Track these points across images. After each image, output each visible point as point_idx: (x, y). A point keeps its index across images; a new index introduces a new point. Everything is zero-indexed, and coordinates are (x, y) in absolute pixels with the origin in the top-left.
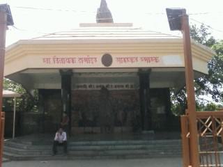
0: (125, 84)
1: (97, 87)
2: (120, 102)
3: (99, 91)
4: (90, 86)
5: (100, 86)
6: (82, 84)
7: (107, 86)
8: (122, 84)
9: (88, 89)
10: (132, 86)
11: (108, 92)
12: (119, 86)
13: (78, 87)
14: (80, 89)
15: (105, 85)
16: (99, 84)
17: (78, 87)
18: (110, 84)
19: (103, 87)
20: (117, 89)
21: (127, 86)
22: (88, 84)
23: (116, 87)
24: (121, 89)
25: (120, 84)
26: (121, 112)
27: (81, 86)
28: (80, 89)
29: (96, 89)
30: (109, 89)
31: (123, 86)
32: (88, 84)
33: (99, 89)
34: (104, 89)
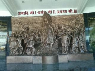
0: (68, 9)
1: (39, 13)
2: (63, 28)
3: (42, 17)
4: (31, 13)
5: (42, 12)
6: (24, 11)
7: (49, 12)
8: (65, 9)
9: (30, 15)
10: (75, 11)
13: (20, 13)
15: (47, 10)
16: (41, 10)
17: (20, 13)
18: (52, 10)
19: (46, 12)
20: (60, 14)
21: (70, 11)
22: (29, 11)
23: (59, 12)
24: (64, 14)
25: (62, 9)
26: (65, 39)
27: (22, 13)
28: (21, 15)
29: (38, 15)
30: (52, 15)
31: (66, 11)
32: (29, 11)
33: (42, 15)
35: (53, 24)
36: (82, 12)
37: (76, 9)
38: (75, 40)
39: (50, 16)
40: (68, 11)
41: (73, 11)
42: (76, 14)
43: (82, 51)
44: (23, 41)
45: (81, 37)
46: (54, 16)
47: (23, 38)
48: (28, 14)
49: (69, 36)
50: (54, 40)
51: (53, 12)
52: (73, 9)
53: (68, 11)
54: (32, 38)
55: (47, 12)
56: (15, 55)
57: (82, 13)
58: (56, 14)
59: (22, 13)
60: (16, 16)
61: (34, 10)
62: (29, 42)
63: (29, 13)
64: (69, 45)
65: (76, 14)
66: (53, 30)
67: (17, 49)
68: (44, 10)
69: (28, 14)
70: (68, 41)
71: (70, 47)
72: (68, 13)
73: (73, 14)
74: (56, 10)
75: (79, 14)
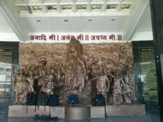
0: (108, 34)
1: (64, 38)
2: (100, 63)
3: (68, 45)
4: (51, 37)
5: (68, 38)
6: (39, 34)
7: (79, 37)
8: (103, 34)
9: (49, 41)
11: (81, 46)
12: (98, 37)
13: (32, 38)
14: (35, 41)
15: (76, 35)
16: (66, 34)
17: (32, 38)
18: (84, 34)
19: (73, 37)
20: (96, 41)
21: (112, 37)
22: (48, 34)
23: (93, 38)
24: (102, 41)
25: (99, 34)
26: (103, 80)
27: (37, 37)
28: (35, 41)
29: (61, 41)
31: (105, 37)
32: (48, 34)
33: (67, 41)
34: (74, 42)
35: (84, 56)
36: (130, 39)
37: (121, 34)
38: (117, 83)
39: (80, 44)
40: (108, 38)
41: (116, 37)
42: (121, 42)
43: (128, 101)
44: (36, 82)
45: (127, 79)
46: (87, 44)
47: (37, 77)
48: (45, 39)
49: (109, 76)
50: (86, 82)
51: (84, 38)
52: (116, 34)
53: (108, 38)
54: (51, 77)
55: (76, 37)
56: (23, 104)
57: (130, 41)
58: (90, 41)
59: (37, 37)
60: (27, 42)
61: (56, 34)
62: (46, 84)
63: (47, 38)
64: (108, 91)
65: (121, 42)
66: (84, 66)
67: (26, 94)
68: (71, 34)
69: (45, 39)
70: (107, 83)
71: (110, 93)
72: (108, 41)
73: (117, 41)
74: (90, 34)
75: (125, 42)
